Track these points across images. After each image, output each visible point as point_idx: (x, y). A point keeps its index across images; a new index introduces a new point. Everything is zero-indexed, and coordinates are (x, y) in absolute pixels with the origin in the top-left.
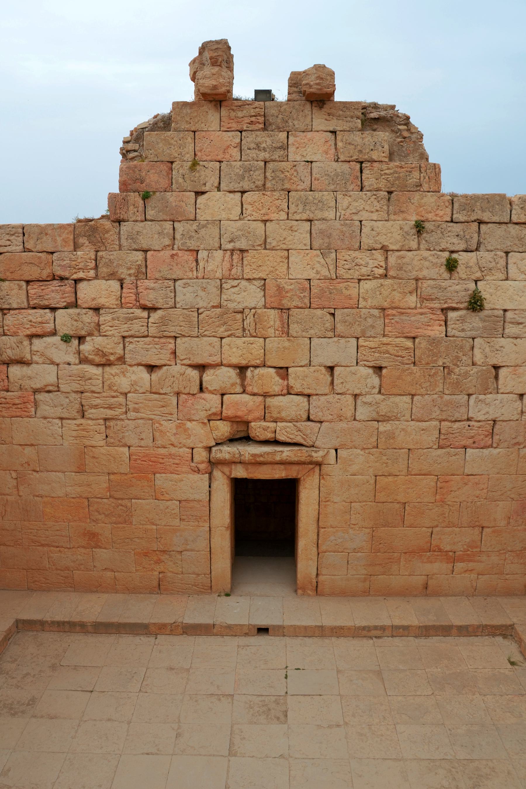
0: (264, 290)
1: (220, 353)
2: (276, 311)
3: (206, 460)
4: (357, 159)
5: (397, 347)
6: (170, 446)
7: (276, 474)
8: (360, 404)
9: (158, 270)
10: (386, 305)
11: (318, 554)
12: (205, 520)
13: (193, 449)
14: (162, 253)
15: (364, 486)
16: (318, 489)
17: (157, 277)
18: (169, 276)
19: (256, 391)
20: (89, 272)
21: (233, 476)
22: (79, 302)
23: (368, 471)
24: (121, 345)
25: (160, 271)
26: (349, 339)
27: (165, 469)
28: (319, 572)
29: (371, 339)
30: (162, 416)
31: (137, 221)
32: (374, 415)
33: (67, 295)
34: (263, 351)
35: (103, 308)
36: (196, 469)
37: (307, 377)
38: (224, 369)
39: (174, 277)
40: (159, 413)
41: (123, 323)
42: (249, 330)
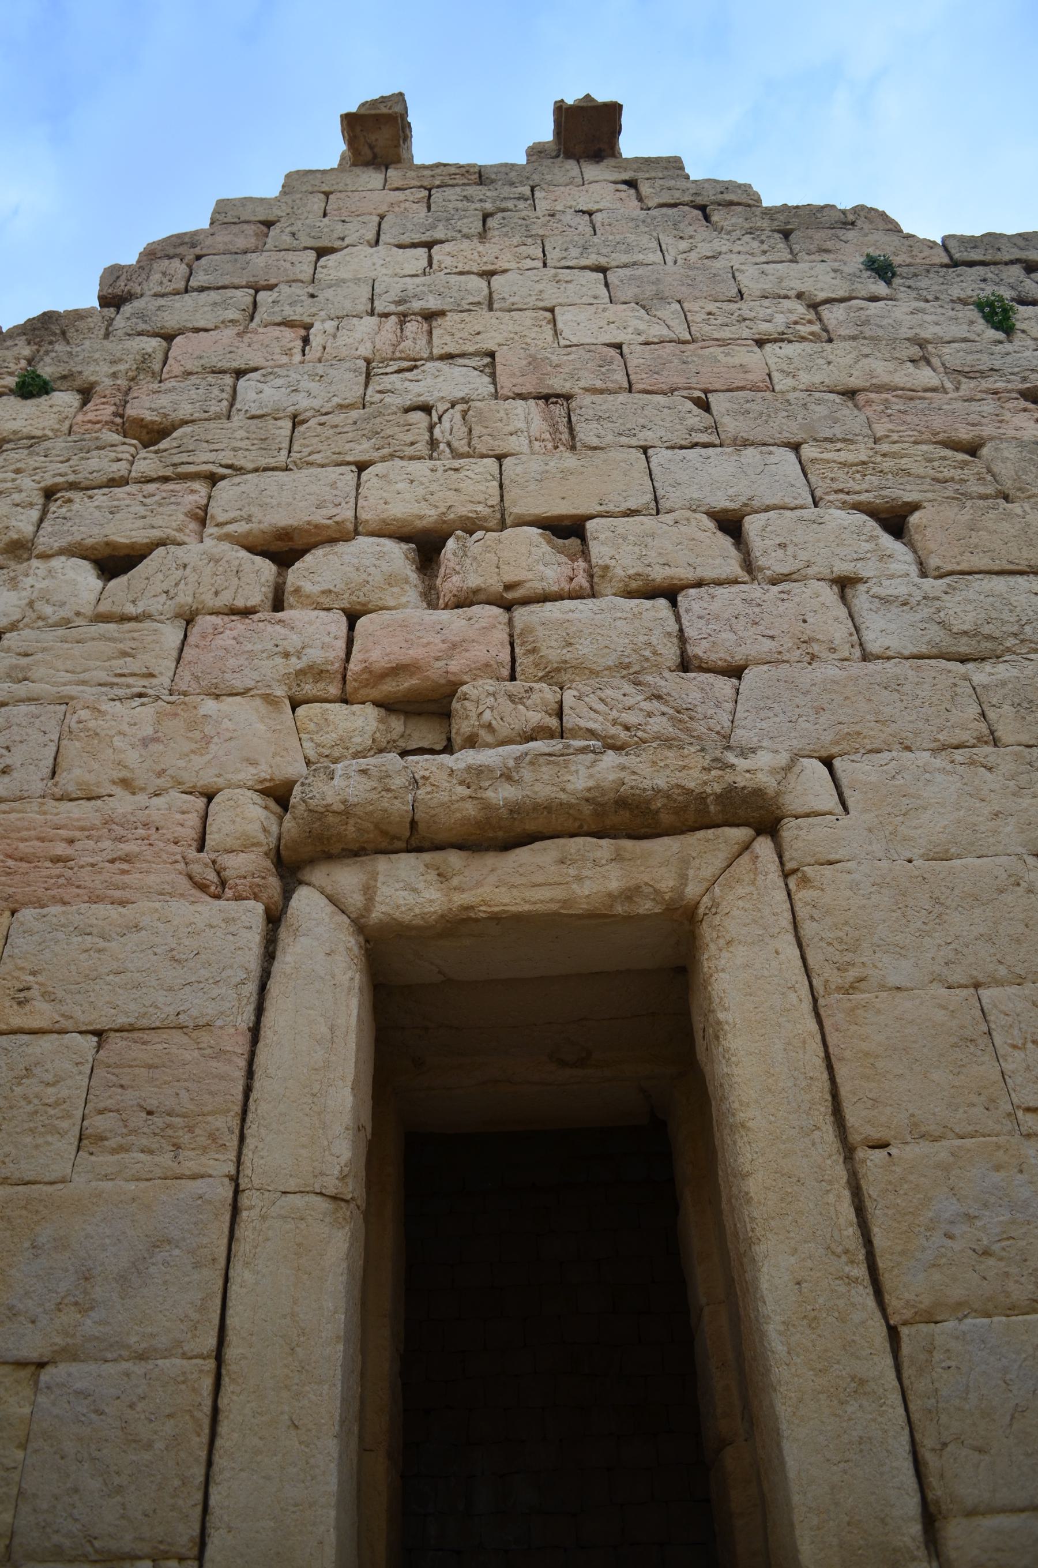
0: (493, 375)
1: (353, 500)
2: (531, 402)
3: (261, 837)
4: (692, 201)
5: (930, 460)
6: (117, 790)
7: (579, 879)
8: (867, 606)
10: (854, 382)
11: (893, 1333)
12: (212, 1137)
13: (210, 797)
15: (1008, 898)
16: (791, 938)
17: (189, 367)
18: (225, 365)
19: (474, 581)
21: (377, 914)
23: (995, 832)
24: (35, 514)
26: (771, 448)
27: (69, 882)
28: (937, 1491)
29: (839, 445)
30: (112, 685)
32: (935, 633)
34: (496, 484)
36: (212, 876)
37: (653, 536)
38: (362, 541)
39: (235, 365)
40: (103, 676)
42: (449, 444)
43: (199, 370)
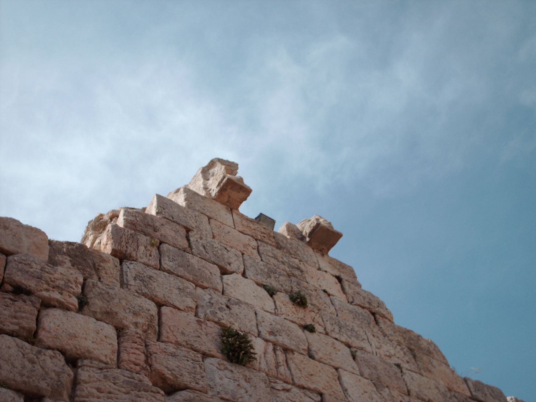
9: (180, 331)
14: (183, 314)
20: (70, 297)
22: (42, 335)
25: (183, 334)
31: (148, 265)
33: (24, 315)
35: (86, 358)
41: (124, 390)
43: (185, 344)
